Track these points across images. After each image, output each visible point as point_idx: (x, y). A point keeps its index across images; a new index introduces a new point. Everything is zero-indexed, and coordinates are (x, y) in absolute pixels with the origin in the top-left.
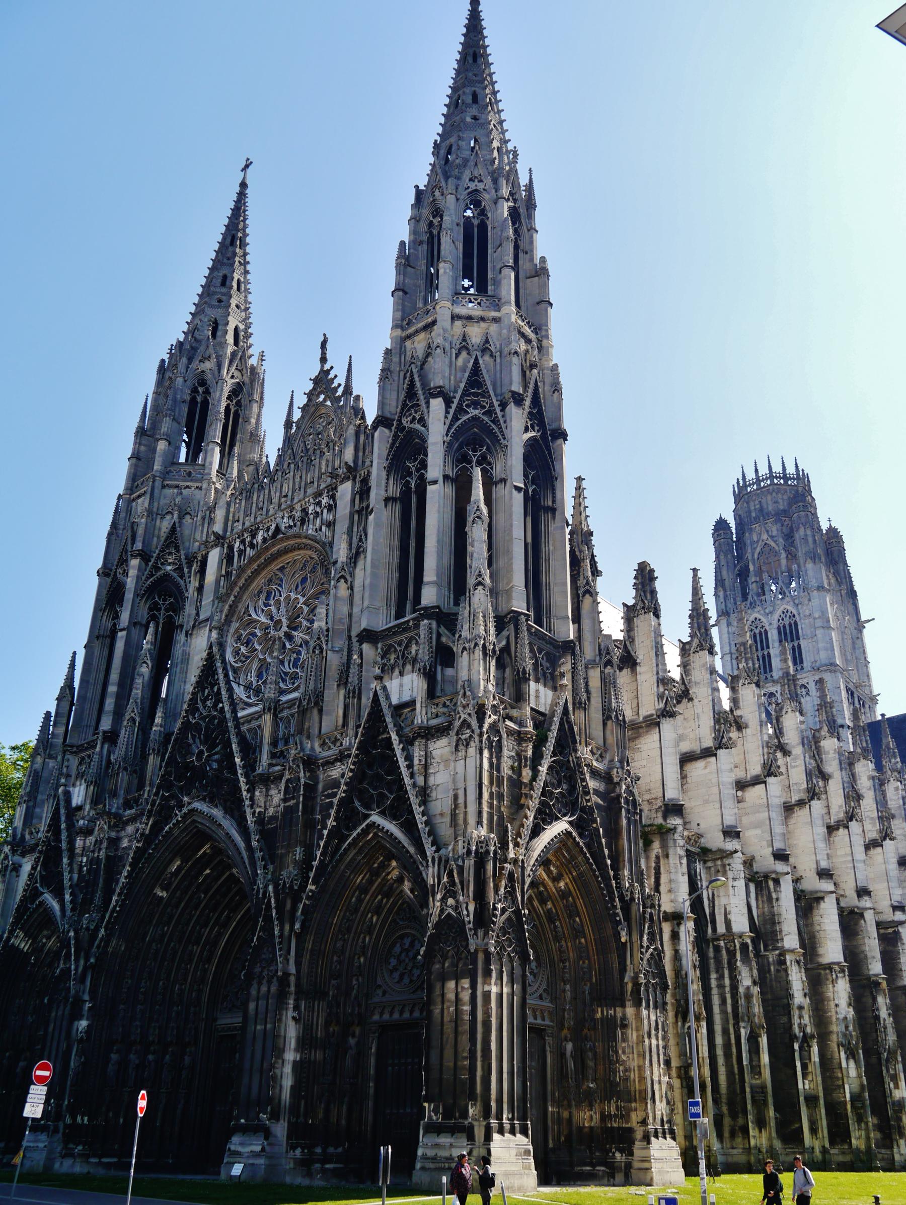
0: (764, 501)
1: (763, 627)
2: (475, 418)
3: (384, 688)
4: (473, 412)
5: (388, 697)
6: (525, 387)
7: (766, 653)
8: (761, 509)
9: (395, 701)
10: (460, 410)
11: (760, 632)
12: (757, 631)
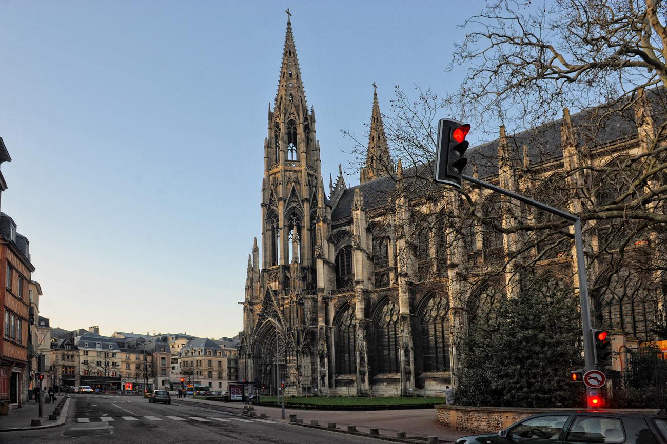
2: (294, 207)
3: (270, 286)
4: (294, 204)
5: (271, 289)
6: (310, 195)
9: (274, 289)
10: (289, 204)
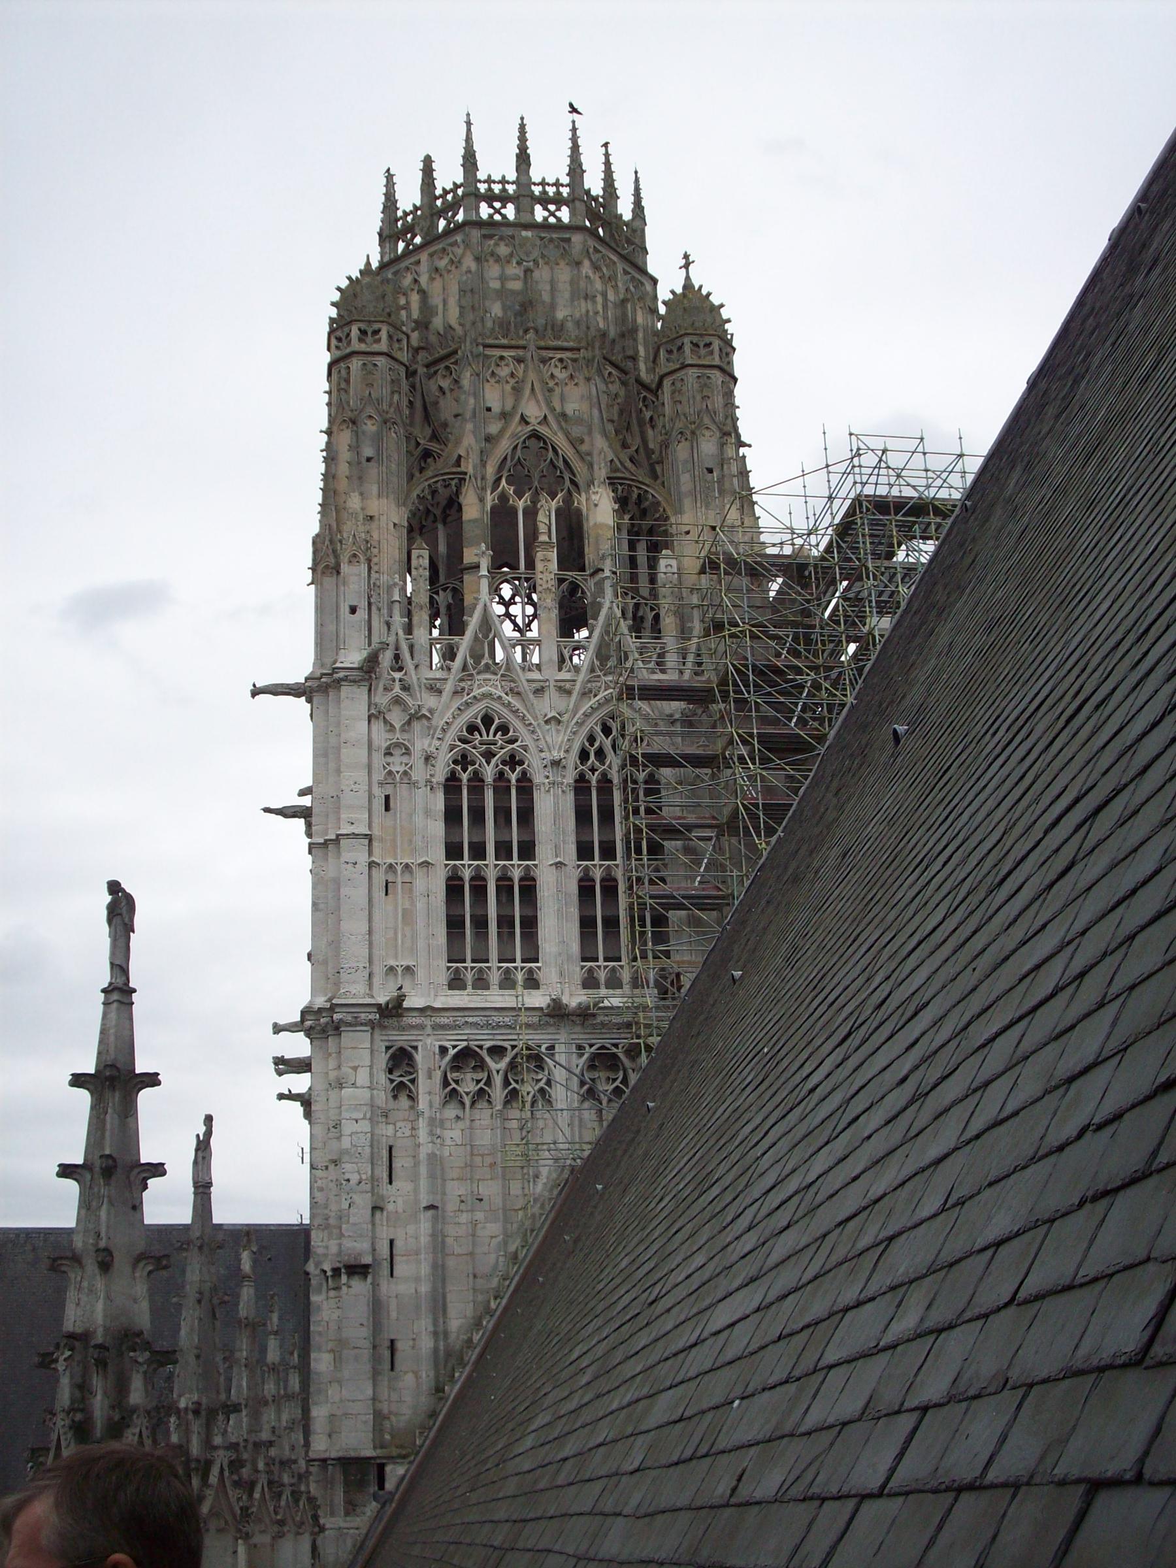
0: (542, 275)
1: (513, 761)
7: (516, 874)
8: (526, 305)
11: (501, 775)
12: (489, 772)
